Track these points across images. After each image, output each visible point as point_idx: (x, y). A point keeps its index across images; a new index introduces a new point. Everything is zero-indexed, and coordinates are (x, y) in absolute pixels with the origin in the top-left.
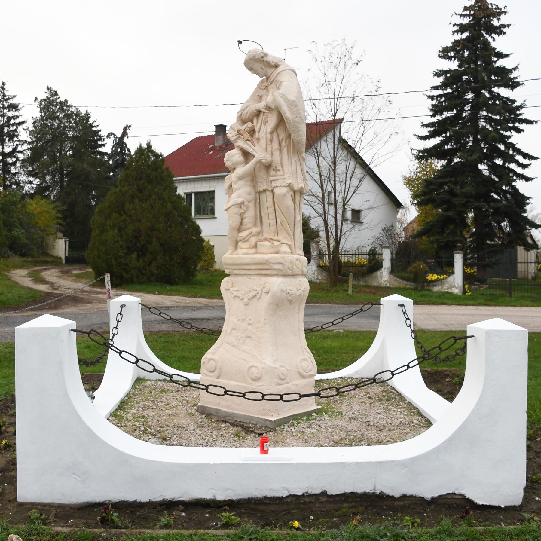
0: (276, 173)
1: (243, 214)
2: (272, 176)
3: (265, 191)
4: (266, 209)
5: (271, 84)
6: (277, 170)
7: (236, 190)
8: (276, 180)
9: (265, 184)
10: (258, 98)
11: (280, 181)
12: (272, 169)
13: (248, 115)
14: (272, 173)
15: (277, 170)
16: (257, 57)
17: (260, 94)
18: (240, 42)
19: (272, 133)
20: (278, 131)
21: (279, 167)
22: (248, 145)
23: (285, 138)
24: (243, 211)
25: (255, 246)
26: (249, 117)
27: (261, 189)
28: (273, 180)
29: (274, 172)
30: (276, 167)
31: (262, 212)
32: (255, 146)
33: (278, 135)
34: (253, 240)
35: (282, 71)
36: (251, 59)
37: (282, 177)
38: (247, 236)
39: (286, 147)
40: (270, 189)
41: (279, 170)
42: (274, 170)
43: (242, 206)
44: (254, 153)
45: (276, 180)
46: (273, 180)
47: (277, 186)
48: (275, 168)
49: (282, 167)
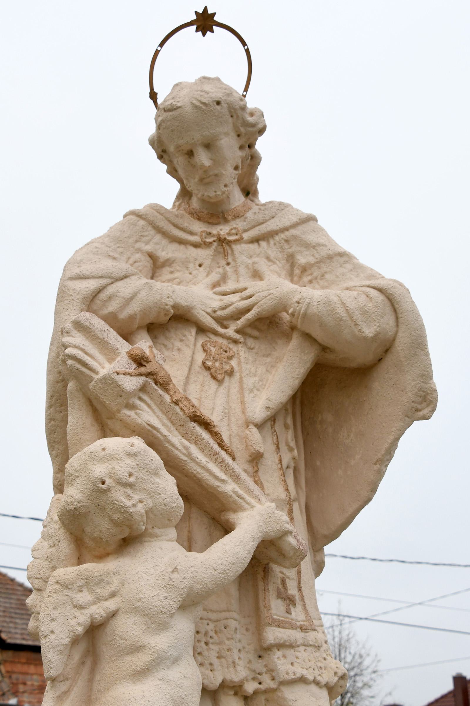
2: (279, 624)
5: (256, 240)
11: (302, 653)
13: (134, 308)
14: (276, 607)
18: (205, 22)
26: (132, 318)
28: (280, 646)
30: (283, 582)
37: (311, 636)
40: (250, 687)
44: (230, 488)
47: (302, 680)
48: (280, 587)
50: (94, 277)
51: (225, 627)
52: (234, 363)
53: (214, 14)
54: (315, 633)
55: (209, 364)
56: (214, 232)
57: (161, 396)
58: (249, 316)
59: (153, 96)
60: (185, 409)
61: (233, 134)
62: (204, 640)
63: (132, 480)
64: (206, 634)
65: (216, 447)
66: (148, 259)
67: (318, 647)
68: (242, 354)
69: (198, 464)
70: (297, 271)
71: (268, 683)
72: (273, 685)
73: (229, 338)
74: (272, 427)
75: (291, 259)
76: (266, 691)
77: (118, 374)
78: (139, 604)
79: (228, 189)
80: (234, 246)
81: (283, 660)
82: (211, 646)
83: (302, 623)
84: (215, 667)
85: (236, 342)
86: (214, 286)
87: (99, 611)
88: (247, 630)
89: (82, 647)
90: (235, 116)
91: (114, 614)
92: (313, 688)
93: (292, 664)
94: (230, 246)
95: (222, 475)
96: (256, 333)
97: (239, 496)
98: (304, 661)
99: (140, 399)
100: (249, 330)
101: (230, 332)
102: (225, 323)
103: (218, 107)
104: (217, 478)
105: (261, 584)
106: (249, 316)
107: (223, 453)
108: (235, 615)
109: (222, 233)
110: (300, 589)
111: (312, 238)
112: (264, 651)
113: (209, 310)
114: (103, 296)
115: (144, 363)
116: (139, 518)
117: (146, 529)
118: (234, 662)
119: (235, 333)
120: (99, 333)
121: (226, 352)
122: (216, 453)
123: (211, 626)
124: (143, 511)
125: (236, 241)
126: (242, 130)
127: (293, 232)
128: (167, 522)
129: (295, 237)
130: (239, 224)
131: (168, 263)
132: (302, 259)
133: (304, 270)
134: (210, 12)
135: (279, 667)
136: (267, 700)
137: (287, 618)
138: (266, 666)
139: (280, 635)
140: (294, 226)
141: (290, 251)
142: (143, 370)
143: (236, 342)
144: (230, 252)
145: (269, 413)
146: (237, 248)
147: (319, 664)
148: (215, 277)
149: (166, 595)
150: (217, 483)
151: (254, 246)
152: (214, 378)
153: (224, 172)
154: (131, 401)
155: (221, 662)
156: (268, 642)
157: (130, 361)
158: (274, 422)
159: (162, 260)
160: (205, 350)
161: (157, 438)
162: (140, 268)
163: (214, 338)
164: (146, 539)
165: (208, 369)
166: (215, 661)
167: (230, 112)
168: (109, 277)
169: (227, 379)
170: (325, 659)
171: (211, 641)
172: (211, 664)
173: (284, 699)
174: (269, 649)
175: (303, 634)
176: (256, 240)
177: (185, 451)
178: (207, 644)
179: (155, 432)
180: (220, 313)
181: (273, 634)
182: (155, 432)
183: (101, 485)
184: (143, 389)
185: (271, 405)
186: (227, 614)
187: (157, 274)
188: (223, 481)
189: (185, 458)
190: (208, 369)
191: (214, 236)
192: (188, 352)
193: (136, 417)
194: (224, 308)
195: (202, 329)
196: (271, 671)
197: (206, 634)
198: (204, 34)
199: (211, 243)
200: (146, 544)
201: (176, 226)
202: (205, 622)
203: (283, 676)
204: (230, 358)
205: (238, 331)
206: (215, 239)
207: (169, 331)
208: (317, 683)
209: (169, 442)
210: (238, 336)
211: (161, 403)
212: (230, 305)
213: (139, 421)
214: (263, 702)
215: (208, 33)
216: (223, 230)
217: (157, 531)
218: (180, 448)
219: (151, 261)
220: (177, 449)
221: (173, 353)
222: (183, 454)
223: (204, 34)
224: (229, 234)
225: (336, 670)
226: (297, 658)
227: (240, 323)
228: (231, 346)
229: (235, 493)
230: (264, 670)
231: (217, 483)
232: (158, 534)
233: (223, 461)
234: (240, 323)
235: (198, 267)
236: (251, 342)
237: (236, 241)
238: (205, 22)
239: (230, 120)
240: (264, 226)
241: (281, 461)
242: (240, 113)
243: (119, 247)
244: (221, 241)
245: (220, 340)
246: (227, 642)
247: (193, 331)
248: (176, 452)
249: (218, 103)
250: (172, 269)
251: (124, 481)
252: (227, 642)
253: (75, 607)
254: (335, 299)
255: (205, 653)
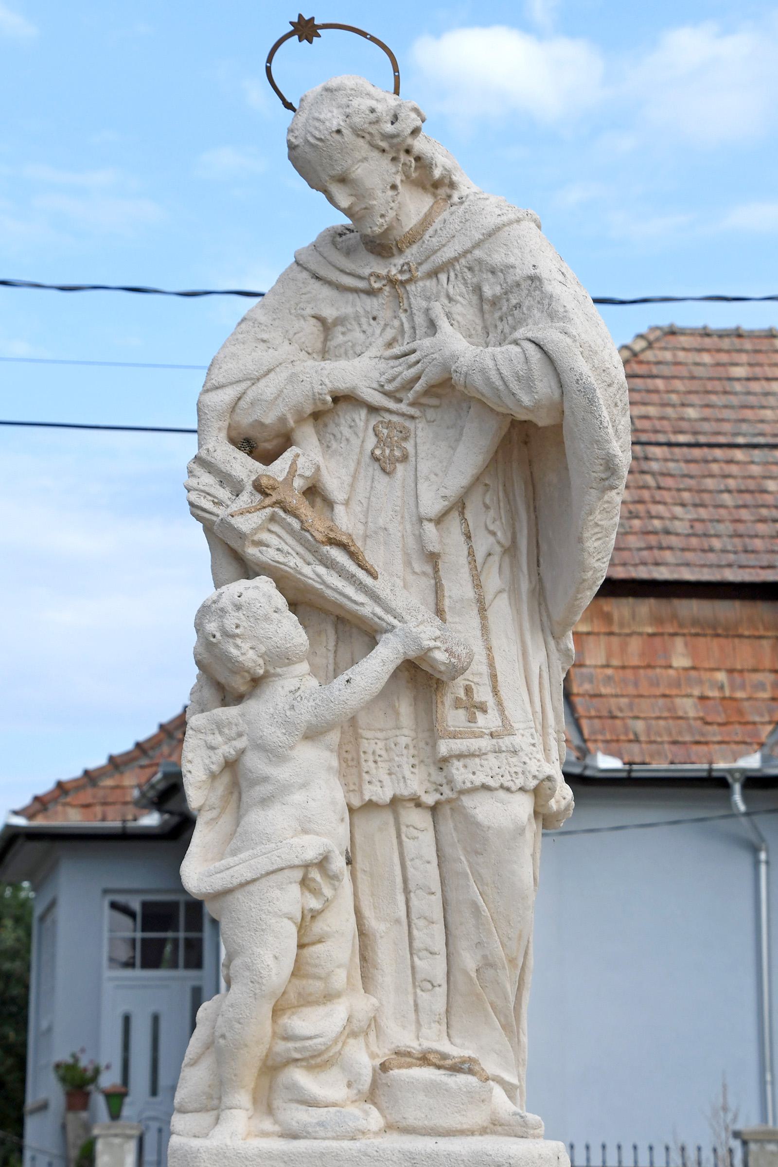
0: (472, 720)
1: (315, 915)
3: (395, 802)
4: (401, 898)
5: (434, 274)
6: (476, 708)
7: (285, 789)
8: (472, 755)
9: (407, 770)
10: (311, 328)
11: (492, 761)
12: (448, 700)
14: (454, 718)
15: (476, 708)
16: (389, 128)
17: (329, 313)
19: (439, 520)
20: (468, 515)
21: (483, 694)
22: (330, 564)
23: (498, 549)
24: (314, 904)
25: (375, 1093)
26: (282, 420)
27: (385, 795)
28: (460, 756)
29: (461, 712)
30: (468, 690)
31: (368, 912)
32: (374, 575)
33: (468, 537)
34: (362, 1059)
35: (510, 223)
36: (359, 133)
37: (506, 742)
38: (335, 1041)
39: (504, 598)
40: (430, 799)
41: (482, 708)
42: (458, 704)
43: (315, 874)
45: (472, 755)
46: (460, 756)
47: (485, 787)
48: (462, 694)
49: (495, 692)
50: (231, 384)
51: (395, 745)
52: (409, 446)
53: (313, 19)
54: (511, 737)
55: (378, 452)
56: (383, 272)
57: (289, 524)
58: (419, 386)
59: (288, 106)
60: (315, 534)
61: (376, 154)
62: (371, 758)
63: (238, 631)
64: (374, 753)
65: (353, 568)
66: (314, 321)
67: (515, 752)
68: (420, 433)
69: (336, 590)
70: (486, 307)
71: (448, 793)
72: (453, 795)
73: (403, 415)
74: (462, 513)
75: (478, 290)
76: (449, 801)
77: (233, 516)
78: (260, 741)
79: (387, 219)
80: (408, 288)
81: (462, 770)
82: (379, 763)
83: (493, 730)
84: (384, 783)
85: (412, 417)
86: (389, 345)
87: (227, 750)
88: (427, 744)
89: (226, 779)
90: (367, 136)
91: (243, 751)
92: (502, 794)
93: (474, 773)
94: (405, 288)
95: (361, 598)
96: (434, 401)
97: (379, 618)
98: (491, 769)
99: (270, 531)
100: (424, 400)
101: (403, 407)
102: (398, 395)
103: (337, 137)
104: (355, 602)
105: (434, 697)
106: (419, 386)
107: (361, 574)
108: (406, 731)
109: (394, 271)
110: (495, 692)
111: (498, 258)
112: (442, 763)
113: (375, 385)
114: (242, 404)
115: (269, 492)
116: (251, 664)
117: (266, 672)
118: (404, 778)
119: (409, 408)
120: (222, 467)
121: (401, 432)
122: (353, 576)
123: (381, 744)
124: (255, 657)
125: (409, 281)
126: (384, 144)
127: (477, 253)
128: (287, 661)
129: (480, 261)
130: (411, 254)
131: (340, 321)
132: (488, 291)
133: (495, 302)
134: (307, 18)
135: (455, 777)
136: (452, 809)
137: (470, 728)
138: (446, 777)
139: (454, 747)
140: (477, 245)
141: (475, 280)
142: (268, 501)
143: (412, 417)
144: (405, 296)
145: (446, 503)
146: (411, 288)
147: (515, 769)
148: (389, 334)
149: (284, 731)
150: (357, 608)
151: (430, 284)
152: (383, 470)
153: (375, 202)
154: (256, 538)
155: (391, 779)
156: (440, 755)
157: (254, 492)
158: (464, 508)
159: (330, 321)
160: (376, 435)
161: (286, 572)
162: (303, 340)
163: (388, 417)
164: (271, 679)
165: (377, 459)
166: (386, 779)
167: (358, 135)
168: (248, 379)
169: (400, 467)
170: (525, 763)
171: (379, 759)
172: (380, 781)
173: (464, 807)
174: (445, 760)
175: (494, 741)
176: (434, 274)
177: (319, 580)
178: (375, 762)
179: (282, 566)
180: (388, 387)
181: (444, 747)
182: (282, 566)
183: (212, 639)
184: (273, 518)
185: (448, 493)
186: (398, 732)
187: (329, 337)
188: (362, 604)
189: (322, 587)
190: (377, 459)
191: (383, 278)
192: (356, 442)
193: (260, 555)
194: (390, 381)
195: (373, 409)
196: (450, 781)
197: (374, 753)
198: (310, 42)
199: (381, 289)
200: (271, 683)
201: (342, 271)
202: (373, 742)
203: (459, 786)
204: (406, 439)
205: (412, 404)
206: (384, 282)
207: (338, 415)
208: (522, 789)
209: (301, 573)
210: (412, 411)
211: (291, 531)
212: (397, 376)
213: (263, 558)
214: (449, 811)
215: (315, 38)
216: (393, 268)
217: (279, 670)
218: (314, 576)
219: (319, 324)
220: (311, 579)
221: (342, 445)
222: (317, 582)
223: (310, 42)
224: (401, 272)
225: (537, 773)
226: (482, 766)
227: (411, 395)
228: (408, 424)
229: (374, 614)
230: (444, 781)
231: (357, 608)
232: (281, 673)
233: (361, 583)
234: (411, 395)
235: (372, 322)
236: (430, 414)
237: (409, 281)
238: (305, 29)
239: (361, 142)
240: (439, 254)
241: (471, 553)
242: (373, 129)
243: (274, 319)
244: (392, 282)
245: (395, 419)
246: (396, 759)
247: (363, 413)
248: (310, 581)
249: (339, 132)
250: (344, 329)
251: (231, 633)
252: (396, 759)
253: (208, 748)
254: (490, 364)
255: (374, 771)
